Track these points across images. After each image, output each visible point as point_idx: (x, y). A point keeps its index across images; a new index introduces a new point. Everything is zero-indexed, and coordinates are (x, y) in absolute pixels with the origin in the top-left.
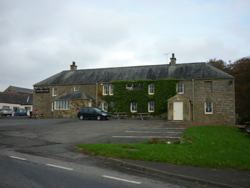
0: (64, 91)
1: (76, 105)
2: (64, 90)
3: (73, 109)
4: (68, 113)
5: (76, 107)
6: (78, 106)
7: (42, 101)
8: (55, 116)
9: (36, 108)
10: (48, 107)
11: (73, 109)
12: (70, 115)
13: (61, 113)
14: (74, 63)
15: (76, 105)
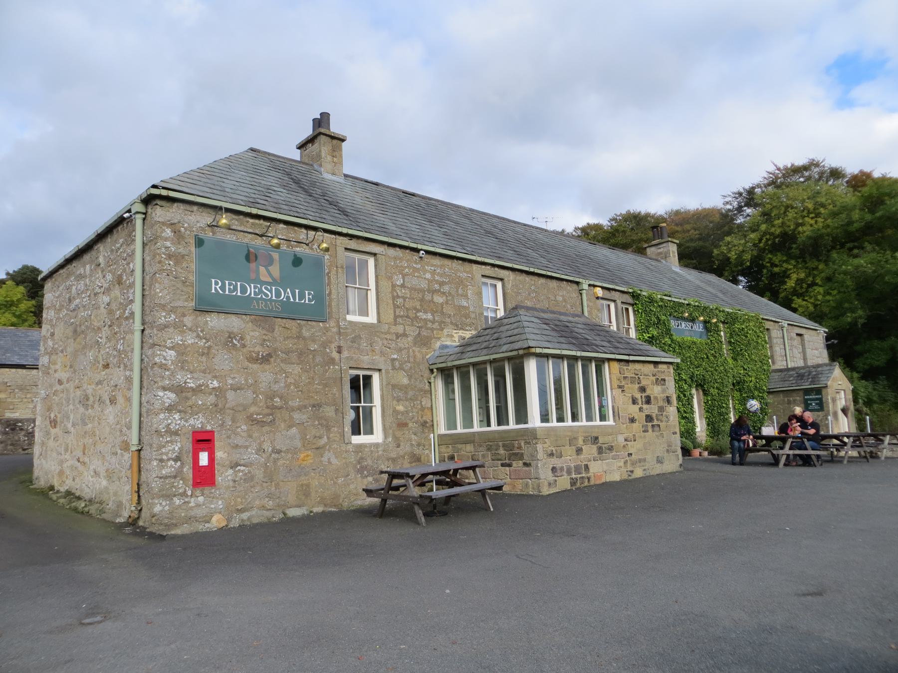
0: (428, 297)
1: (638, 395)
2: (424, 285)
3: (632, 420)
4: (611, 448)
5: (641, 409)
6: (648, 401)
7: (262, 351)
8: (550, 477)
9: (198, 422)
10: (317, 406)
11: (632, 420)
12: (622, 464)
13: (579, 451)
14: (321, 122)
15: (638, 395)
